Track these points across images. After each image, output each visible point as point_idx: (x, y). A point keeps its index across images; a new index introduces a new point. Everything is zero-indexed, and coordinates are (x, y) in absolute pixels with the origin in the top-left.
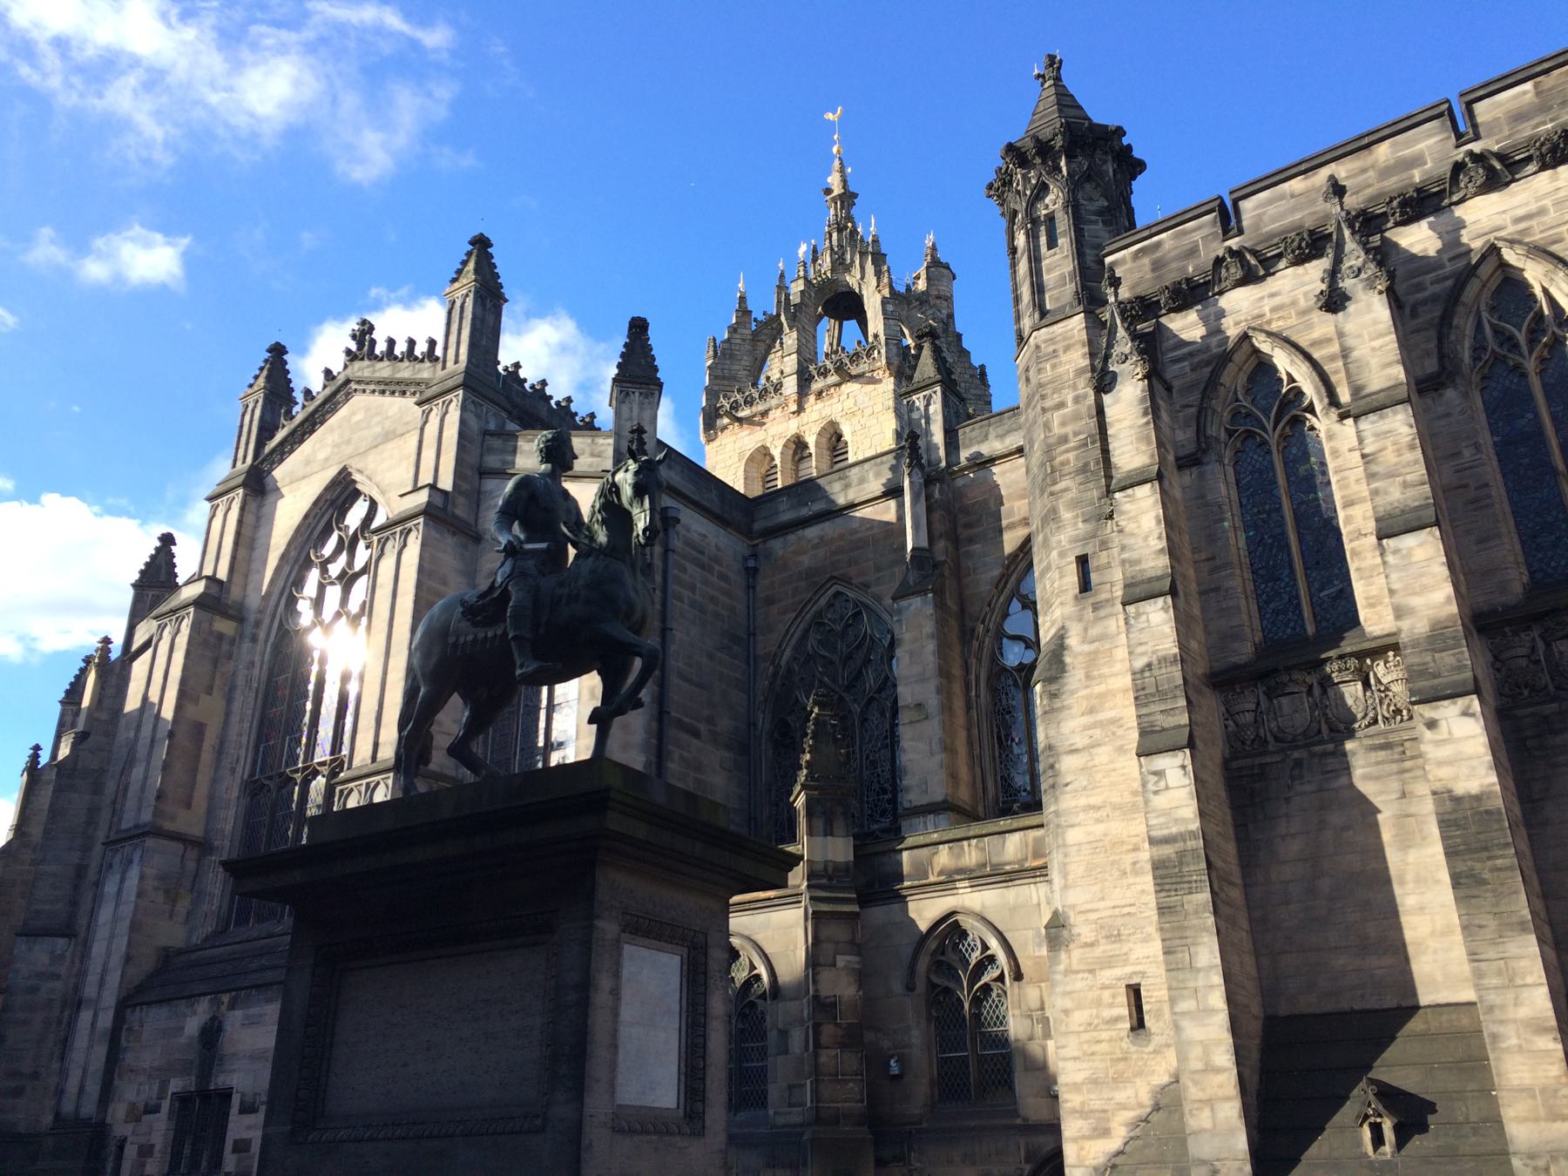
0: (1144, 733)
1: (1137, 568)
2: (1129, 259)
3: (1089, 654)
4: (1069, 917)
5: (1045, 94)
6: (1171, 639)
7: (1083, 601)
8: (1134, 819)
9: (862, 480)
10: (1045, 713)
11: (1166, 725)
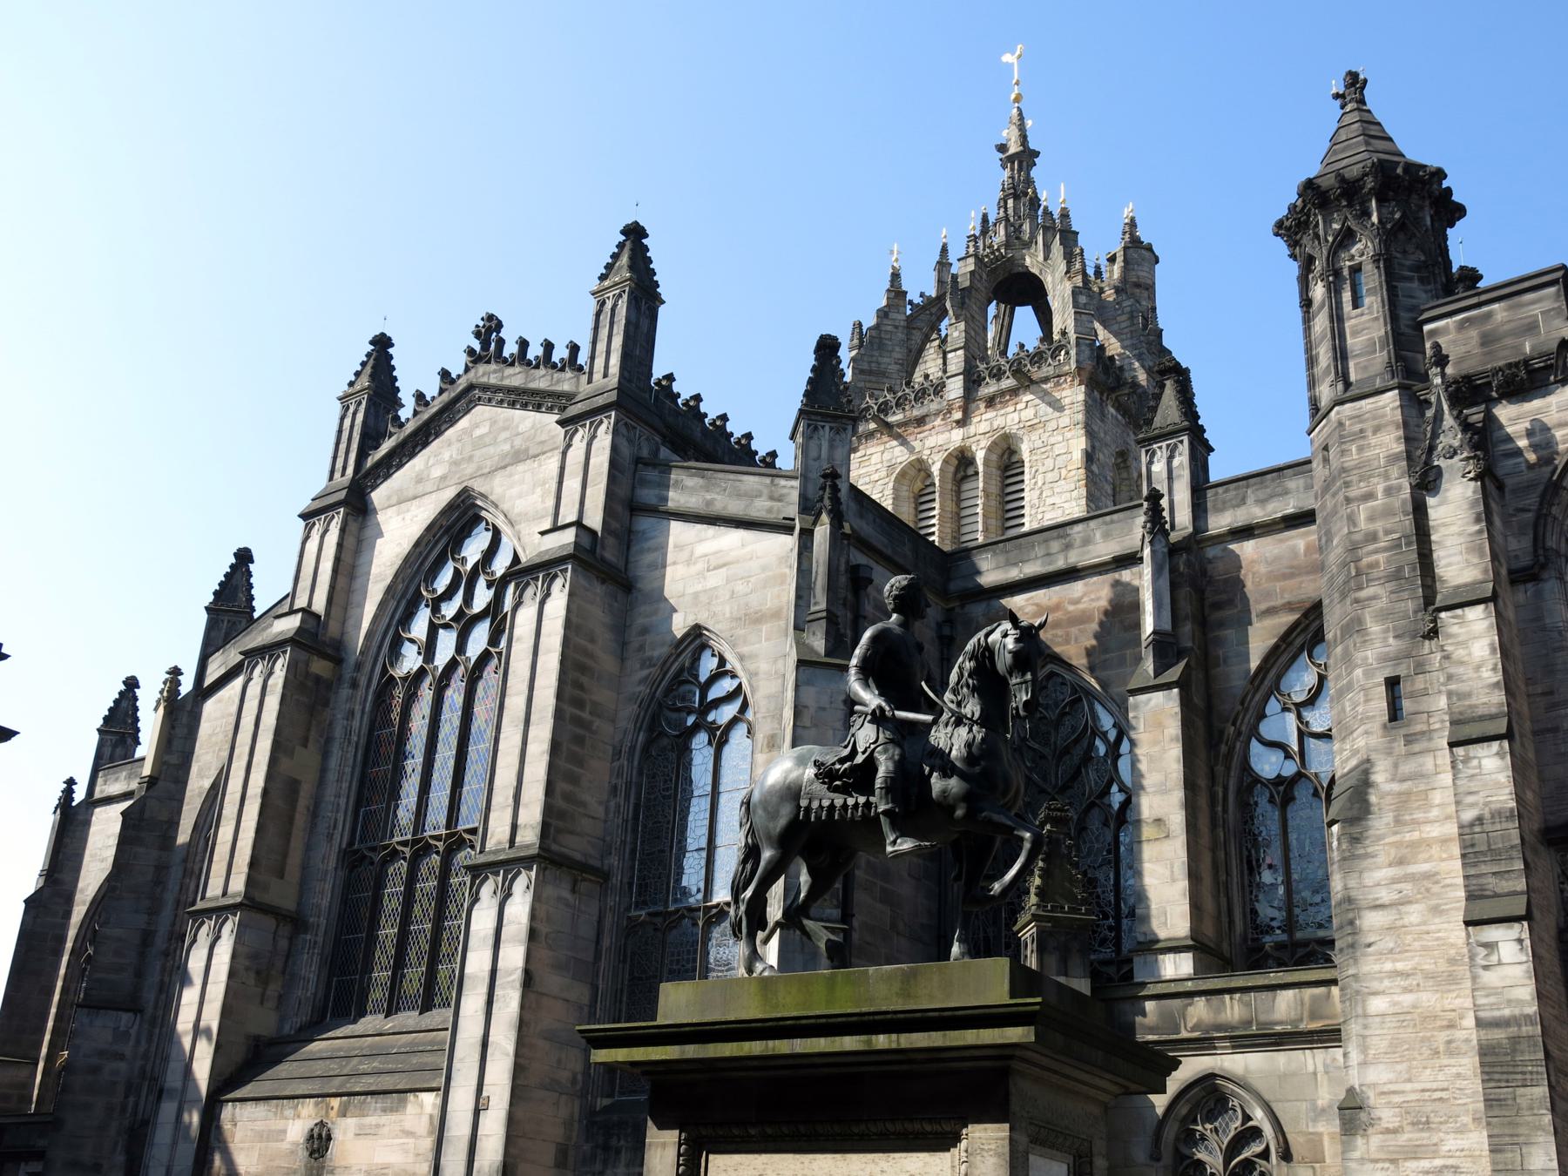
0: (1471, 897)
1: (1467, 703)
2: (1451, 327)
3: (1400, 794)
4: (1368, 1098)
5: (1348, 119)
6: (1507, 791)
7: (1394, 732)
8: (1449, 991)
9: (1087, 541)
10: (1344, 859)
11: (1498, 890)
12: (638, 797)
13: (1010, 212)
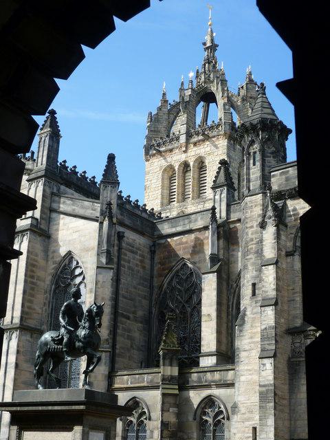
0: (262, 350)
9: (196, 220)
13: (207, 69)
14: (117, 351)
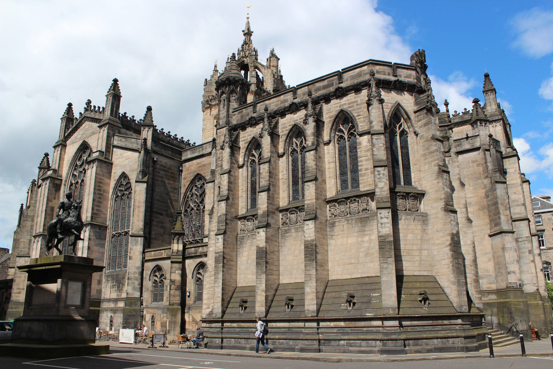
9: (206, 148)
12: (114, 209)
13: (244, 48)
14: (153, 236)
